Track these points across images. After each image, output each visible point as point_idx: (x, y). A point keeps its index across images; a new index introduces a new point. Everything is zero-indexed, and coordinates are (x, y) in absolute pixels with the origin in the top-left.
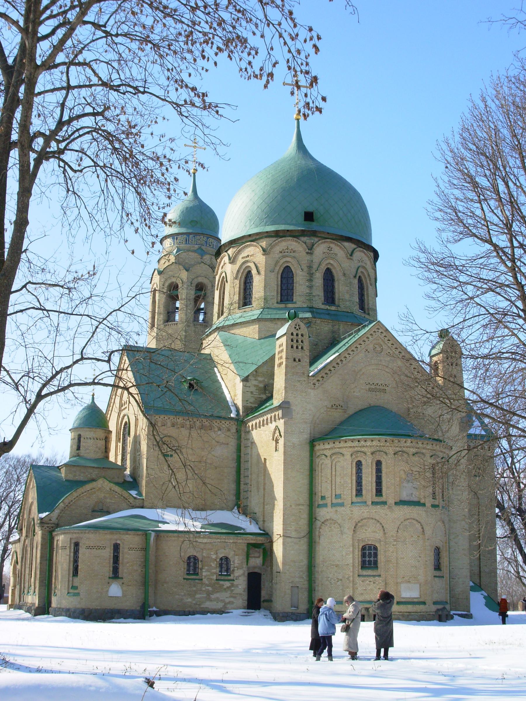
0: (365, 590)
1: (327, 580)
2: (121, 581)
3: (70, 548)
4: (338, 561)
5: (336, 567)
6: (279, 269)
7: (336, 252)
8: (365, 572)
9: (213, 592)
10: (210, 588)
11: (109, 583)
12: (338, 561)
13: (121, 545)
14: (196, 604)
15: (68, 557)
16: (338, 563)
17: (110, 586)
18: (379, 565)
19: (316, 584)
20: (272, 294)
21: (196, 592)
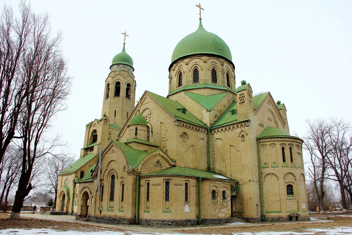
0: (290, 205)
2: (189, 204)
3: (163, 184)
4: (277, 192)
5: (276, 195)
6: (211, 69)
8: (289, 198)
10: (220, 206)
13: (188, 184)
14: (216, 215)
15: (162, 190)
16: (276, 193)
18: (294, 194)
19: (264, 203)
20: (209, 79)
21: (216, 209)
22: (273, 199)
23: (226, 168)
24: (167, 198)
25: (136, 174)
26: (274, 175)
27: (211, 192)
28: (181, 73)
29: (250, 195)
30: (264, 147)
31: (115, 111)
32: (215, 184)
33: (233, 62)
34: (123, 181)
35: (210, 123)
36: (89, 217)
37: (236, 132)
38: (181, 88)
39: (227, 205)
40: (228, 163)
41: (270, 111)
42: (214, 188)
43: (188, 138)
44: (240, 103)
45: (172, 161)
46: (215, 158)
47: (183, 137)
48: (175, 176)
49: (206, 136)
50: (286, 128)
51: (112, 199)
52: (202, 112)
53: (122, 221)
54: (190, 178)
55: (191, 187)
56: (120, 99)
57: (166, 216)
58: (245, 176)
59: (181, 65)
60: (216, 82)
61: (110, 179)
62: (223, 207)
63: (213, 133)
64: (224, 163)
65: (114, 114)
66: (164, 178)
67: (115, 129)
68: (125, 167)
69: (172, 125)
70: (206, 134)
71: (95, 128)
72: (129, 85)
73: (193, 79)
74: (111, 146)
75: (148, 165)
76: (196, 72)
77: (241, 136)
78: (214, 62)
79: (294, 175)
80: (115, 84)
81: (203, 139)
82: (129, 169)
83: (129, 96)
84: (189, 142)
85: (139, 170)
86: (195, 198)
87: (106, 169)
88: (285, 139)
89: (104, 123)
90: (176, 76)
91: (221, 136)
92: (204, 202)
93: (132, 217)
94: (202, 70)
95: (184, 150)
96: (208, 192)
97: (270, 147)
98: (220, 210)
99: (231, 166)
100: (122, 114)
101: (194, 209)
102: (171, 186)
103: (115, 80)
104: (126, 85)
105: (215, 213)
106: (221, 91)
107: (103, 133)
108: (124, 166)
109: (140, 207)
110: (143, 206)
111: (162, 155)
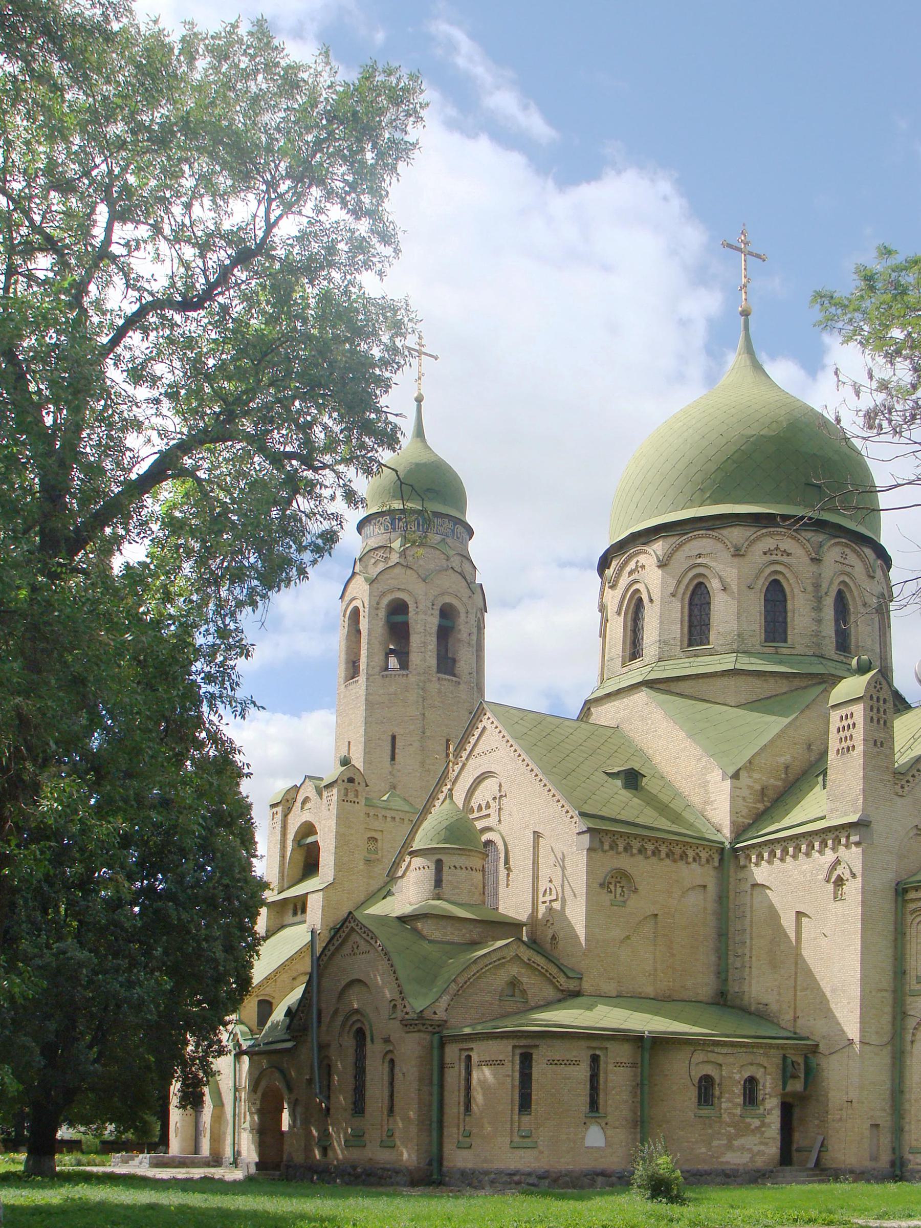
3: (513, 1062)
7: (852, 564)
9: (737, 1136)
10: (732, 1130)
13: (602, 1058)
14: (712, 1157)
15: (509, 1080)
17: (587, 1129)
23: (779, 994)
24: (525, 1103)
25: (430, 1029)
27: (696, 1082)
28: (640, 600)
31: (390, 738)
32: (712, 1057)
34: (391, 1048)
35: (733, 823)
36: (288, 1167)
38: (637, 672)
39: (763, 1124)
42: (709, 1070)
45: (568, 977)
49: (712, 873)
51: (359, 1107)
52: (708, 777)
53: (391, 1178)
55: (610, 1067)
56: (412, 679)
57: (521, 1158)
59: (640, 564)
61: (349, 1042)
62: (743, 1130)
63: (742, 863)
65: (389, 752)
66: (515, 1042)
67: (393, 818)
68: (395, 1006)
71: (306, 816)
72: (447, 614)
73: (686, 630)
74: (347, 930)
78: (777, 549)
80: (382, 613)
81: (705, 886)
82: (407, 1013)
83: (454, 661)
84: (638, 905)
85: (441, 1015)
86: (627, 1102)
87: (336, 1012)
89: (346, 795)
93: (419, 1163)
96: (683, 1081)
99: (795, 987)
100: (423, 749)
102: (539, 1069)
103: (383, 594)
104: (438, 612)
106: (797, 683)
107: (342, 840)
108: (393, 1003)
109: (445, 1134)
110: (455, 1130)
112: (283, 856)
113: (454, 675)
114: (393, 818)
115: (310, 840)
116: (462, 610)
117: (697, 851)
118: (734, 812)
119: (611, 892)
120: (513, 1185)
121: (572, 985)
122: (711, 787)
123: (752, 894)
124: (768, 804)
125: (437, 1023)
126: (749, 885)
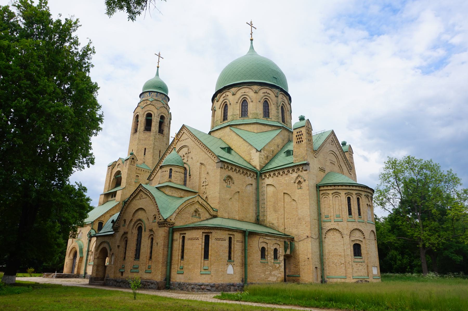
0: (358, 270)
1: (333, 264)
2: (233, 264)
3: (202, 238)
5: (339, 256)
6: (262, 101)
8: (356, 260)
9: (273, 270)
11: (227, 264)
12: (340, 252)
13: (233, 239)
14: (266, 278)
15: (200, 246)
17: (228, 267)
18: (363, 255)
19: (325, 266)
20: (260, 112)
22: (336, 261)
23: (278, 220)
24: (206, 256)
25: (169, 226)
26: (337, 232)
27: (260, 249)
28: (226, 104)
29: (307, 255)
30: (325, 196)
32: (265, 240)
33: (289, 93)
34: (152, 233)
35: (260, 165)
36: (107, 280)
37: (292, 178)
39: (280, 266)
40: (281, 214)
41: (333, 153)
42: (264, 245)
43: (233, 183)
44: (297, 142)
45: (213, 210)
46: (266, 208)
47: (227, 181)
48: (216, 228)
49: (254, 180)
50: (352, 175)
51: (137, 256)
52: (251, 152)
53: (149, 285)
54: (235, 231)
55: (235, 242)
56: (152, 134)
57: (204, 278)
58: (301, 231)
59: (227, 95)
60: (269, 117)
61: (135, 232)
63: (263, 177)
64: (276, 214)
65: (144, 153)
66: (203, 231)
67: (144, 171)
68: (155, 217)
69: (214, 167)
70: (255, 179)
71: (119, 169)
72: (162, 118)
73: (241, 112)
74: (138, 191)
75: (184, 215)
76: (244, 103)
77: (297, 182)
79: (362, 232)
80: (145, 116)
81: (252, 184)
82: (160, 220)
83: (163, 131)
84: (234, 188)
85: (173, 221)
87: (132, 220)
88: (351, 188)
89: (131, 163)
90: (221, 108)
91: (273, 181)
92: (251, 262)
93: (161, 280)
94: (252, 101)
95: (228, 197)
96: (257, 249)
97: (333, 197)
98: (271, 272)
99: (284, 218)
100: (153, 152)
101: (239, 269)
103: (146, 111)
104: (160, 117)
105: (265, 276)
106: (273, 128)
107: (129, 175)
108: (155, 216)
109: (172, 268)
110: (176, 266)
111: (201, 203)
112: (110, 181)
113: (163, 134)
114: (144, 171)
115: (119, 176)
116: (166, 118)
117: (250, 173)
118: (260, 162)
119: (226, 183)
120: (201, 290)
121: (214, 213)
122: (252, 155)
123: (267, 188)
124: (269, 161)
125: (172, 224)
126: (266, 185)
